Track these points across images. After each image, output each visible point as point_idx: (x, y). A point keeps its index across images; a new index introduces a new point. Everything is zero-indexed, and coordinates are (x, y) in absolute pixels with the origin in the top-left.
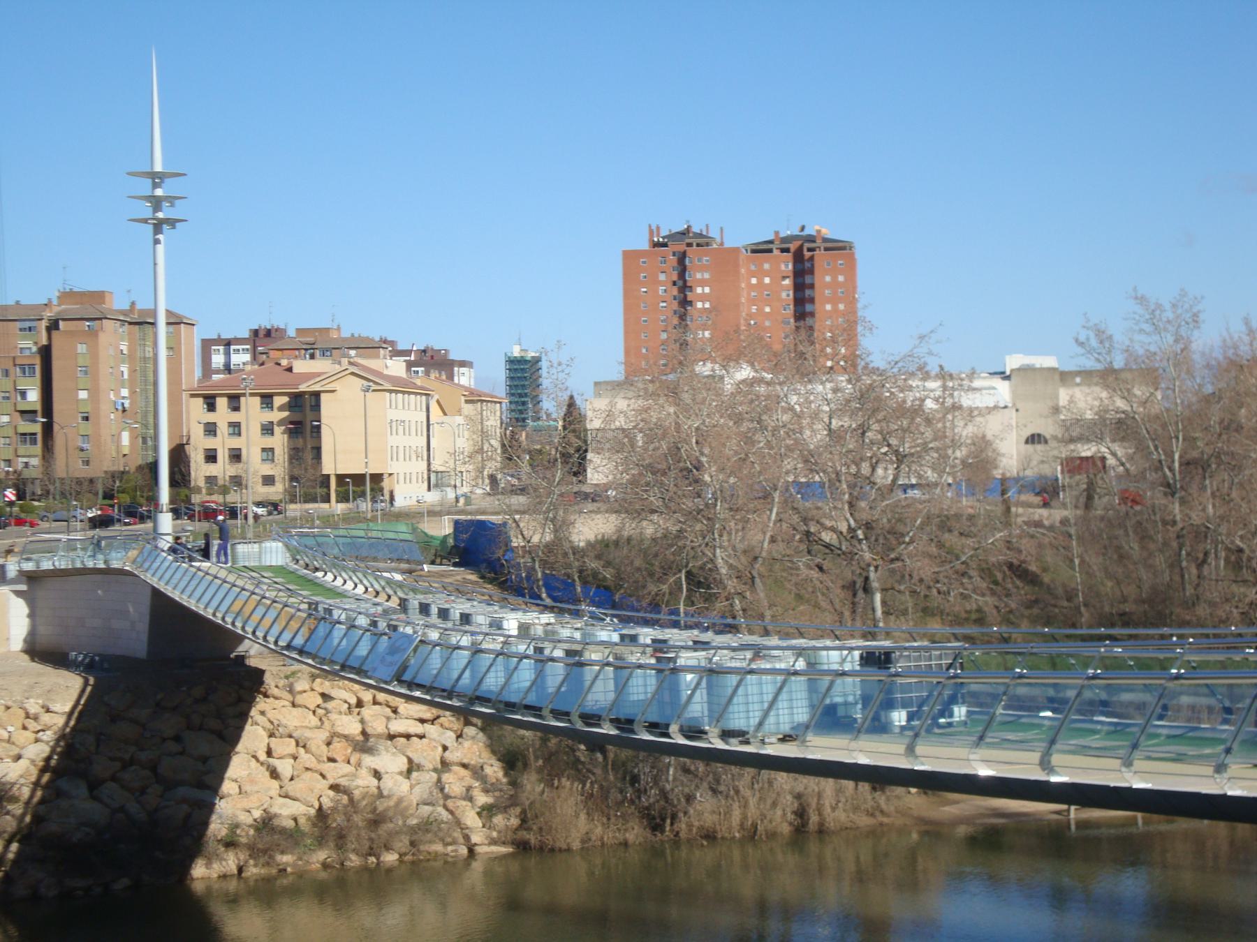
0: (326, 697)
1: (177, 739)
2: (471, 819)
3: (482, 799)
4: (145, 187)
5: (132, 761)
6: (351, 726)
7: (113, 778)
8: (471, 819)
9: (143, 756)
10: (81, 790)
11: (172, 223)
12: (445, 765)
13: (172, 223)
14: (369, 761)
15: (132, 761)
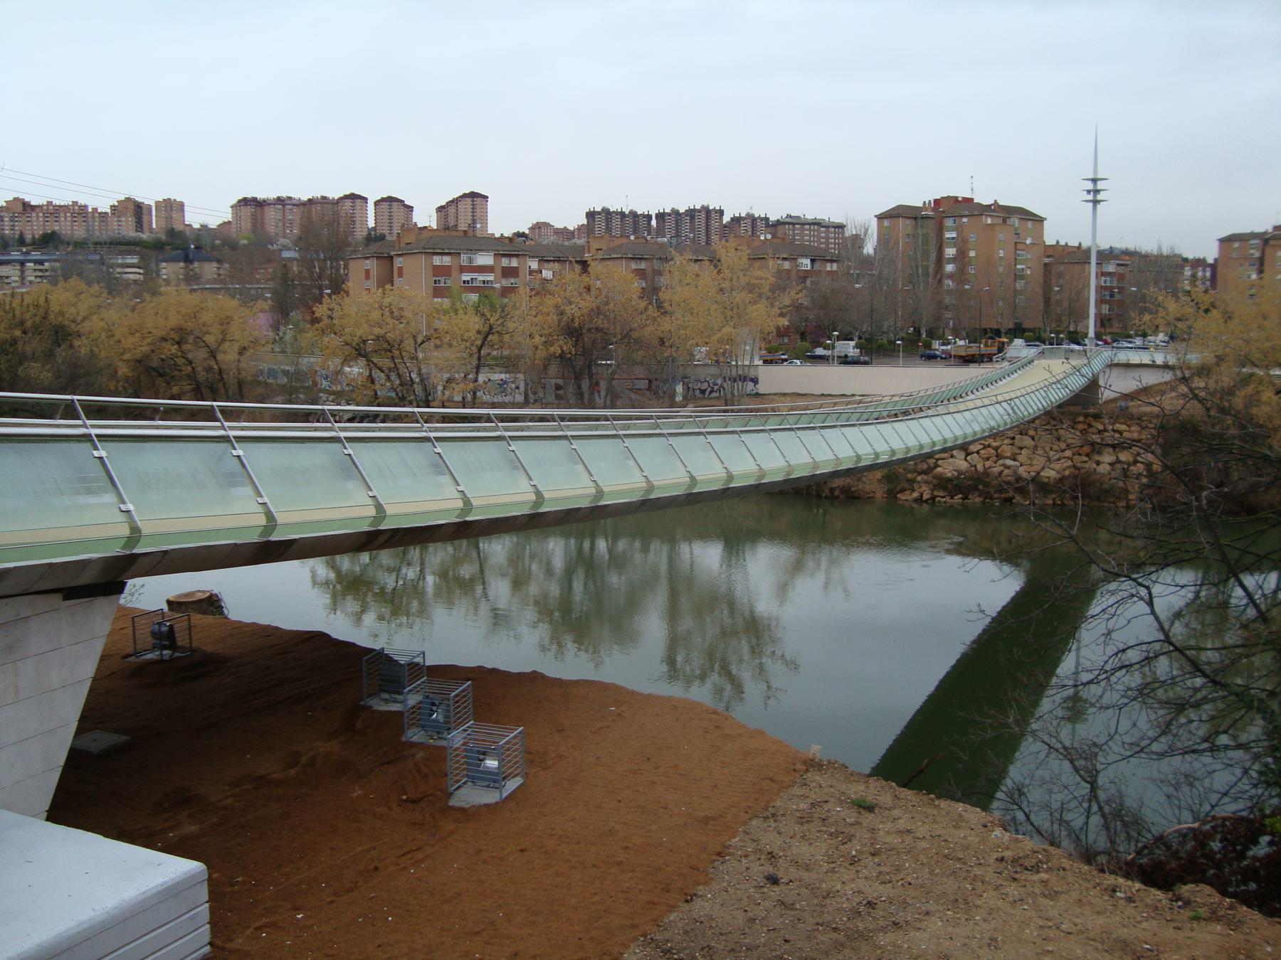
0: (1090, 426)
1: (1013, 438)
2: (1134, 487)
3: (1144, 480)
4: (1090, 186)
5: (989, 446)
6: (1096, 438)
7: (978, 452)
8: (1134, 487)
9: (994, 444)
10: (962, 455)
11: (1099, 202)
12: (1135, 462)
13: (1099, 202)
14: (1097, 457)
15: (989, 446)
